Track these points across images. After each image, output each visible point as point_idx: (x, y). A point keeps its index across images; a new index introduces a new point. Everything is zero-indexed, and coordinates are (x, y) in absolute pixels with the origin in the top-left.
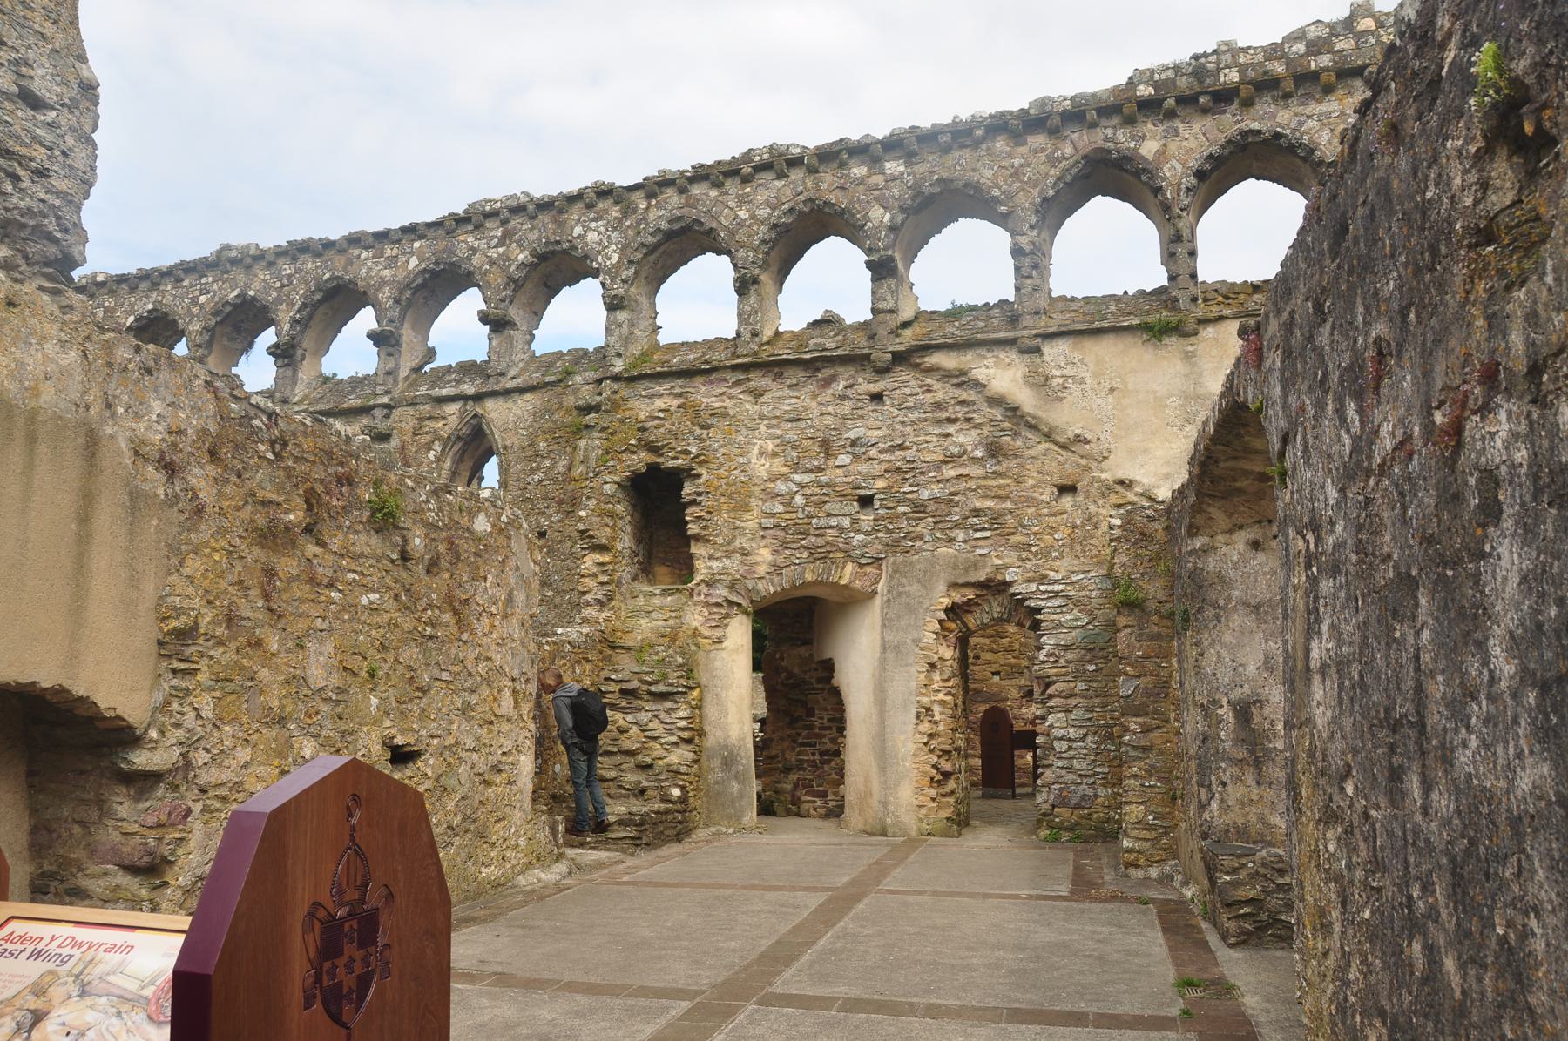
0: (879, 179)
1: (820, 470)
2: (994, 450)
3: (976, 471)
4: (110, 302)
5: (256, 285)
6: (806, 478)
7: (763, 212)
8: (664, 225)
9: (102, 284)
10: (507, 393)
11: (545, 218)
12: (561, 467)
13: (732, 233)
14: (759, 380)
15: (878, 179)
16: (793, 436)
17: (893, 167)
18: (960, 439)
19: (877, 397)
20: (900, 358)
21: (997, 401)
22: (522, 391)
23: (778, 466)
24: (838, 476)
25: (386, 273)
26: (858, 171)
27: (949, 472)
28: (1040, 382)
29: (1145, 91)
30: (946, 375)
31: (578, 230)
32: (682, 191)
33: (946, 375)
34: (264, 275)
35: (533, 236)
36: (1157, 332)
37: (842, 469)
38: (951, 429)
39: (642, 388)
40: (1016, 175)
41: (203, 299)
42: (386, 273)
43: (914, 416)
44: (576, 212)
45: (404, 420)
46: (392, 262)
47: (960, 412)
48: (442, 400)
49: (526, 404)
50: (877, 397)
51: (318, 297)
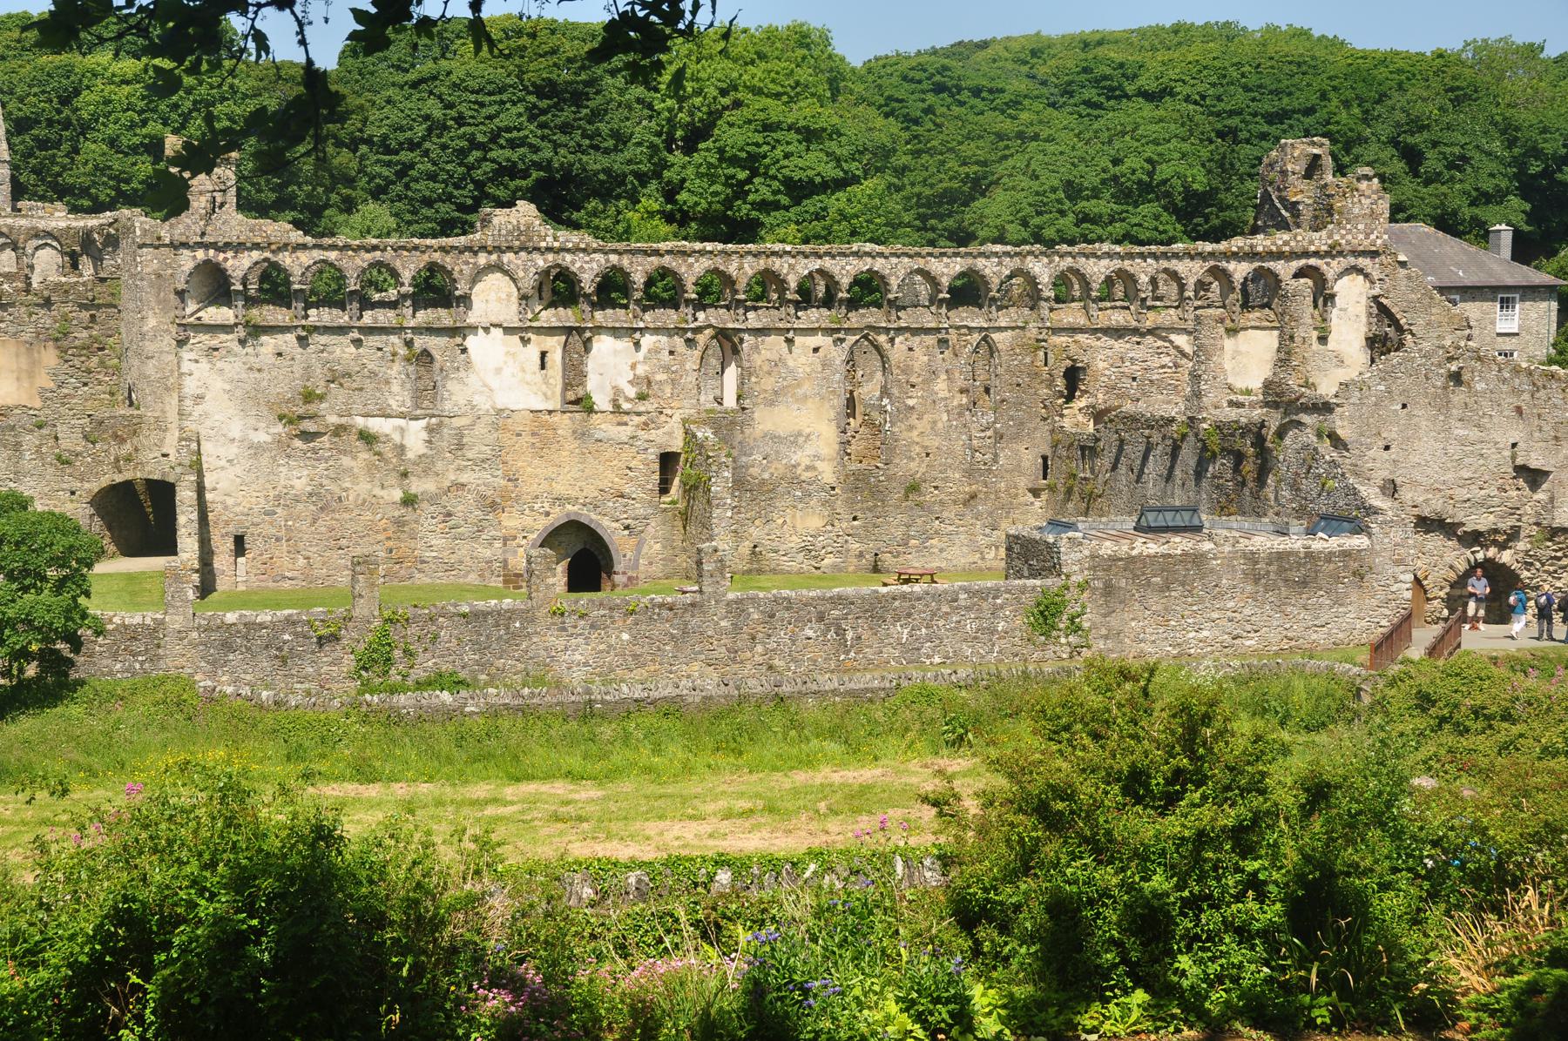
2: (1176, 366)
4: (792, 261)
7: (1103, 270)
11: (1017, 259)
12: (1028, 360)
19: (1138, 343)
20: (1151, 332)
21: (1177, 348)
22: (1006, 329)
23: (1105, 365)
37: (1128, 368)
41: (848, 268)
42: (945, 270)
44: (1029, 258)
46: (947, 265)
49: (1009, 333)
50: (1138, 343)
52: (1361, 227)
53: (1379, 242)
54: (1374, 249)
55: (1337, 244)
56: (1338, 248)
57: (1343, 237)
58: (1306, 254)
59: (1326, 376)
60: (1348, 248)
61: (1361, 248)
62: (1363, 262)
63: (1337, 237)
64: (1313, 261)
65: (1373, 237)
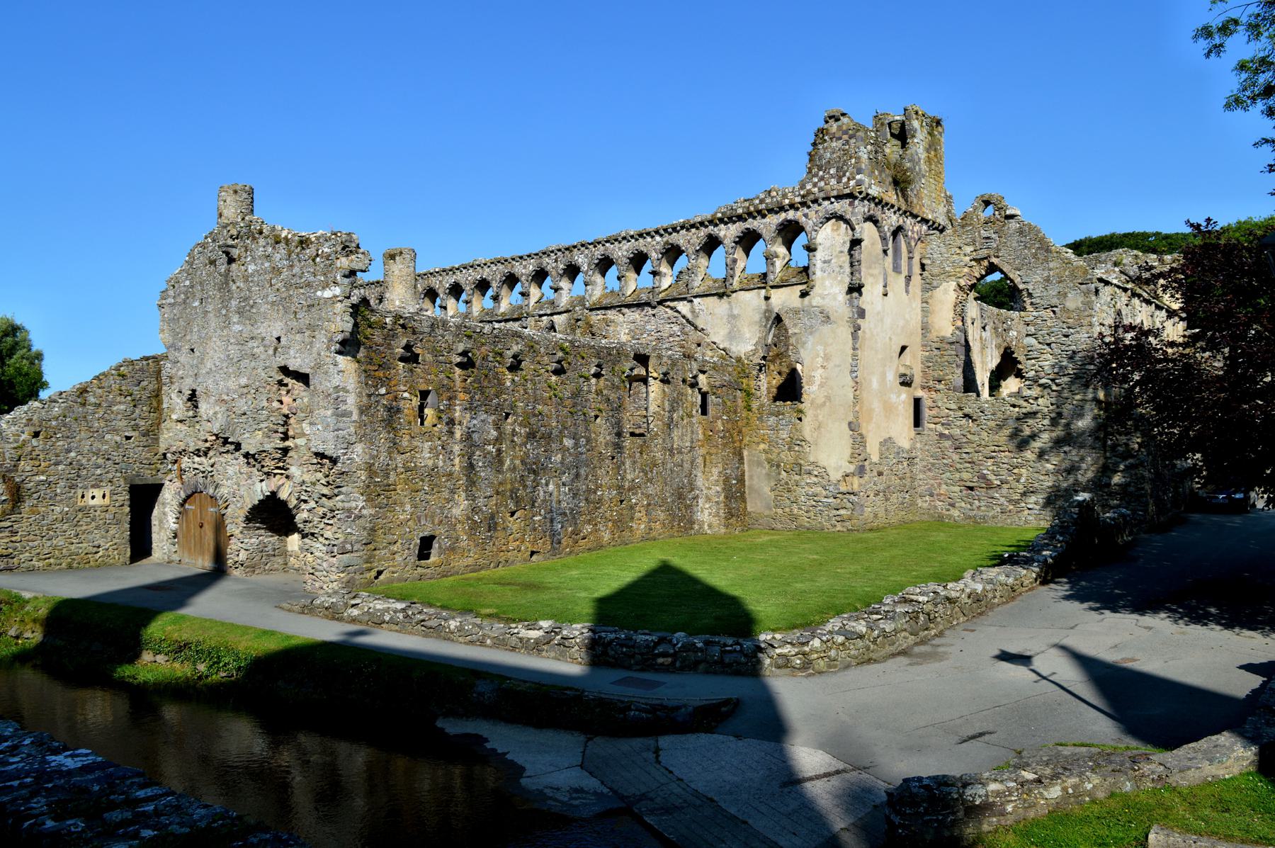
0: (654, 243)
1: (639, 339)
3: (677, 339)
4: (440, 278)
5: (485, 274)
6: (636, 341)
7: (625, 253)
8: (600, 257)
9: (437, 272)
10: (559, 313)
13: (617, 260)
14: (625, 310)
15: (654, 243)
16: (633, 328)
17: (658, 238)
18: (674, 329)
20: (661, 303)
24: (643, 341)
25: (523, 271)
26: (649, 239)
27: (671, 339)
28: (693, 312)
29: (719, 215)
30: (672, 308)
31: (576, 258)
32: (603, 245)
33: (668, 307)
34: (487, 270)
35: (564, 260)
36: (721, 296)
38: (672, 325)
39: (594, 313)
40: (689, 242)
41: (469, 278)
42: (523, 271)
43: (663, 321)
45: (531, 321)
46: (525, 267)
47: (674, 320)
48: (541, 316)
50: (654, 315)
51: (504, 278)
52: (832, 171)
53: (852, 183)
54: (847, 191)
55: (809, 192)
56: (812, 197)
57: (815, 185)
58: (782, 209)
59: (811, 333)
60: (822, 195)
61: (835, 193)
62: (840, 207)
63: (809, 186)
64: (791, 215)
65: (845, 180)
